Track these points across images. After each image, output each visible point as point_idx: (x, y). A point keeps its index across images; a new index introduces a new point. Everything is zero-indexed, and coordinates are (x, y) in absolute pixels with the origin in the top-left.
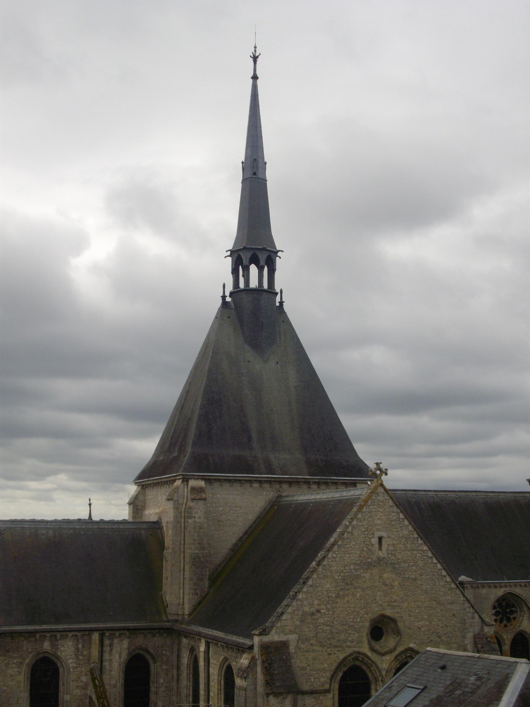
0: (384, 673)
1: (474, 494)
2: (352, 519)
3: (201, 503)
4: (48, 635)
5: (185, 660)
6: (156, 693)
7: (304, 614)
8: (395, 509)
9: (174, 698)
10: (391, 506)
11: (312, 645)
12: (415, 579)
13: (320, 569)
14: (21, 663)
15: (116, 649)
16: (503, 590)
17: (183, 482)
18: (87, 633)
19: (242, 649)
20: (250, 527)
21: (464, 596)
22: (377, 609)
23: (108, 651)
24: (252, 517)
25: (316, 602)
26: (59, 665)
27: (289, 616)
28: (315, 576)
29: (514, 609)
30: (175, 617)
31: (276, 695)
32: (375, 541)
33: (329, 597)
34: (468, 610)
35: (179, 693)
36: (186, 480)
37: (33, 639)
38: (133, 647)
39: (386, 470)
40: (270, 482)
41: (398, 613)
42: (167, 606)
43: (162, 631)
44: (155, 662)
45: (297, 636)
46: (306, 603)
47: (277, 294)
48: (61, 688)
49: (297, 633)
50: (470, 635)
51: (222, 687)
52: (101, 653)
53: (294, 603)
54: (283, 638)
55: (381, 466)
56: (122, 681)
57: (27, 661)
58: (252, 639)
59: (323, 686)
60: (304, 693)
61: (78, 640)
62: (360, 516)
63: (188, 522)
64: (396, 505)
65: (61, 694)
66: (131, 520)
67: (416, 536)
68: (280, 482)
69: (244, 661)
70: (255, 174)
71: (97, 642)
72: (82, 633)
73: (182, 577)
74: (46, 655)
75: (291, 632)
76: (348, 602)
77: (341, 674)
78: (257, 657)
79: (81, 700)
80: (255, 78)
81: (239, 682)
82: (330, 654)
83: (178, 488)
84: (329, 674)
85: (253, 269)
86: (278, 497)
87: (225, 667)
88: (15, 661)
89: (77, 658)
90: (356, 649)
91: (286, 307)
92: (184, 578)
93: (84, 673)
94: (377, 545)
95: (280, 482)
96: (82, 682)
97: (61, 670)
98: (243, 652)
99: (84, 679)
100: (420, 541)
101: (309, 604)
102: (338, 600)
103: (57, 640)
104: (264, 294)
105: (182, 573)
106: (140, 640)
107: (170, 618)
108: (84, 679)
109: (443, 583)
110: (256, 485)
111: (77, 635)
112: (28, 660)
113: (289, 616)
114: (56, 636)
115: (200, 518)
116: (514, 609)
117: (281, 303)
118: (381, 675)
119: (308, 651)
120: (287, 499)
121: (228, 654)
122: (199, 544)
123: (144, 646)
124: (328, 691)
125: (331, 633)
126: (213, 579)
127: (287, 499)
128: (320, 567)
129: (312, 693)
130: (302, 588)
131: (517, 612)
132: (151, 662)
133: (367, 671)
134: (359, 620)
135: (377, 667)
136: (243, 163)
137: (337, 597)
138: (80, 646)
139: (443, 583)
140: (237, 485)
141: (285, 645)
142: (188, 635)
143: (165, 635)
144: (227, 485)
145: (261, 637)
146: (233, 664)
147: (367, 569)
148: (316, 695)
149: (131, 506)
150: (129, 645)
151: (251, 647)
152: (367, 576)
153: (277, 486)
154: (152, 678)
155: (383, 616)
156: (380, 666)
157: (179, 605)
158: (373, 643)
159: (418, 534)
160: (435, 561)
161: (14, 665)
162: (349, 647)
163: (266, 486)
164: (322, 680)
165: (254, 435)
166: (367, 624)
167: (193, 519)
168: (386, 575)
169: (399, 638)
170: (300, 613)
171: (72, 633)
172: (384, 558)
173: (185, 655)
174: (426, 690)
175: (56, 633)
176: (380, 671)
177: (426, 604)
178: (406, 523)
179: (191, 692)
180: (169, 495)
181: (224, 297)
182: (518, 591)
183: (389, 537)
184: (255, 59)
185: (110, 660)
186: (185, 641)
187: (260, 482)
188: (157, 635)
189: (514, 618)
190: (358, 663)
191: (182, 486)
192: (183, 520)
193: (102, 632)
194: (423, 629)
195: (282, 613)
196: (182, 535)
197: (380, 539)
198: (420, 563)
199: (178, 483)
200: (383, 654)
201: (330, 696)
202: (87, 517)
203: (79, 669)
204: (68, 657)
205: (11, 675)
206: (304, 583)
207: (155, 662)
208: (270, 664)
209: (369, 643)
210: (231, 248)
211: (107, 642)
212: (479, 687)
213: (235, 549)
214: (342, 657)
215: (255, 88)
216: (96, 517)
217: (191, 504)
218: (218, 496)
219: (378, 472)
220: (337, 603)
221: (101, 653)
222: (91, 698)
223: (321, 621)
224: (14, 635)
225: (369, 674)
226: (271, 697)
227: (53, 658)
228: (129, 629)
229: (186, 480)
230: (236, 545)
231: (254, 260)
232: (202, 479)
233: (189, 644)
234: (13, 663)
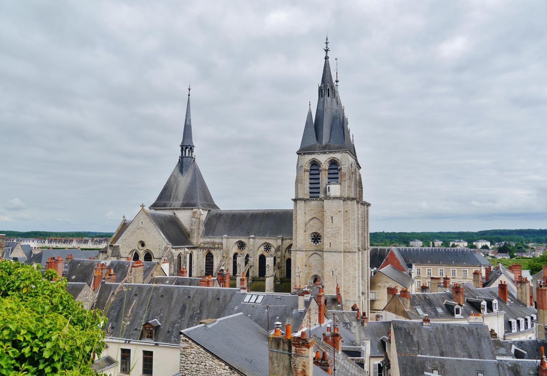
7: (123, 239)
50: (164, 247)
54: (118, 245)
75: (120, 243)
80: (189, 95)
104: (184, 158)
141: (118, 246)
152: (138, 231)
165: (172, 197)
168: (142, 231)
182: (243, 240)
184: (189, 89)
189: (244, 249)
198: (152, 228)
215: (189, 98)
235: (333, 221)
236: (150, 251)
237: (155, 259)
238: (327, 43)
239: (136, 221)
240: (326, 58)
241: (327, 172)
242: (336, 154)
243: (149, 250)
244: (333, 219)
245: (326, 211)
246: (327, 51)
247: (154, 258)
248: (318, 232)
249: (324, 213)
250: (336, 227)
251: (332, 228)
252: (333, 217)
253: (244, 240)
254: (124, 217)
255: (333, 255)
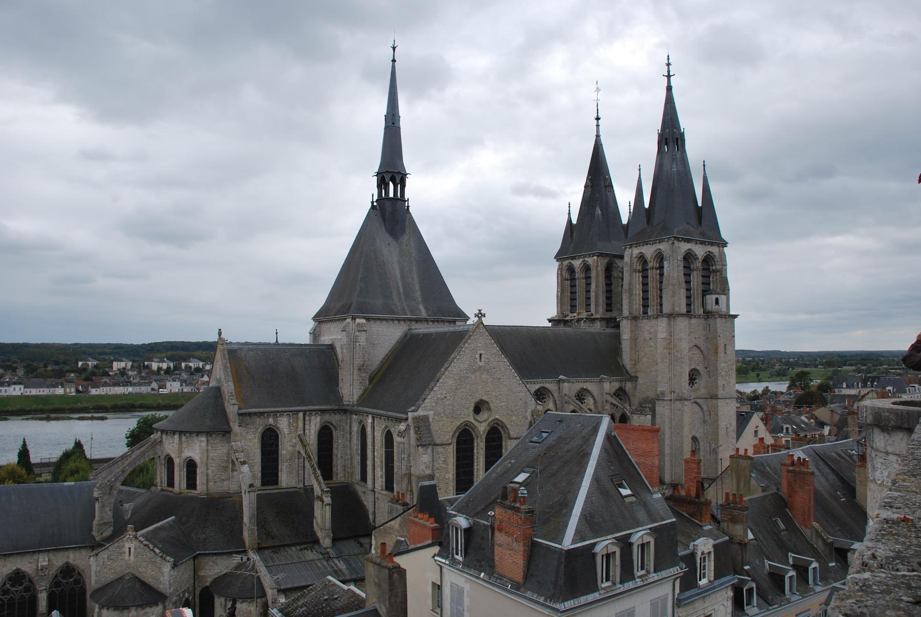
0: (482, 433)
1: (521, 328)
2: (465, 343)
3: (363, 333)
4: (272, 414)
5: (355, 428)
6: (337, 449)
7: (438, 399)
8: (490, 337)
9: (348, 451)
10: (487, 336)
11: (442, 417)
12: (499, 379)
13: (447, 373)
14: (256, 432)
15: (313, 422)
16: (539, 385)
17: (352, 320)
18: (295, 413)
19: (400, 420)
20: (392, 348)
21: (527, 388)
22: (478, 396)
23: (308, 424)
24: (393, 342)
25: (444, 392)
26: (278, 432)
27: (429, 401)
28: (444, 377)
29: (544, 396)
30: (348, 403)
31: (423, 446)
32: (478, 356)
33: (451, 389)
34: (528, 396)
35: (351, 448)
36: (354, 319)
37: (262, 417)
38: (323, 421)
39: (485, 314)
40: (404, 320)
41: (490, 398)
42: (343, 397)
43: (340, 411)
44: (336, 430)
45: (433, 412)
46: (438, 393)
47: (406, 201)
48: (280, 446)
49: (433, 410)
50: (529, 411)
51: (384, 443)
52: (304, 424)
53: (432, 393)
54: (426, 413)
55: (482, 312)
56: (316, 442)
57: (259, 430)
58: (407, 414)
59: (448, 440)
60: (438, 445)
61: (290, 417)
62: (469, 341)
63: (356, 345)
64: (490, 335)
65: (280, 450)
66: (312, 343)
67: (501, 353)
68: (411, 320)
69: (402, 427)
70: (393, 124)
71: (302, 418)
72: (293, 413)
73: (352, 378)
74: (271, 426)
75: (430, 410)
76: (462, 392)
77: (458, 434)
78: (411, 424)
79: (293, 453)
80: (394, 61)
81: (397, 439)
82: (452, 422)
83: (349, 323)
84: (451, 434)
85: (391, 185)
86: (409, 330)
87: (385, 431)
88: (252, 430)
89: (289, 428)
90: (467, 419)
91: (411, 209)
92: (353, 379)
93: (294, 437)
94: (479, 359)
95: (411, 320)
96: (293, 442)
97: (280, 436)
98: (401, 422)
99: (294, 441)
100: (503, 356)
101: (440, 393)
102: (457, 391)
103: (277, 417)
104: (399, 201)
105: (352, 376)
106: (327, 417)
107: (345, 403)
108: (294, 441)
109: (515, 381)
110: (396, 322)
111: (289, 414)
112: (260, 430)
113: (429, 401)
114: (276, 415)
115: (363, 342)
116: (544, 396)
117: (408, 207)
118: (480, 434)
119: (440, 421)
120: (416, 331)
121: (390, 423)
122: (362, 358)
123: (329, 421)
124: (450, 444)
125: (453, 410)
126: (371, 380)
127: (416, 331)
128: (447, 372)
129: (442, 445)
130: (436, 384)
131: (546, 398)
132: (333, 430)
133: (472, 432)
134: (468, 402)
135: (478, 429)
136: (385, 116)
137: (455, 389)
138: (291, 421)
139: (515, 381)
140: (384, 322)
141: (426, 418)
142: (357, 413)
143: (342, 414)
144: (378, 322)
145: (413, 413)
146: (392, 430)
147: (473, 373)
148: (444, 446)
149: (312, 335)
150: (321, 420)
151: (407, 419)
152: (473, 376)
153: (409, 323)
154: (334, 440)
155: (481, 400)
156: (479, 429)
157: (350, 395)
158: (475, 415)
159: (502, 352)
160: (511, 368)
161: (251, 433)
162: (463, 418)
163: (402, 323)
164: (447, 437)
166: (473, 405)
167: (359, 343)
168: (483, 376)
169: (490, 413)
170: (435, 398)
171: (287, 413)
172: (483, 366)
173: (355, 426)
174: (553, 432)
175: (276, 413)
176: (479, 432)
177: (506, 393)
178: (495, 345)
179: (360, 448)
180: (343, 328)
181: (372, 202)
182: (547, 386)
183: (485, 354)
184: (394, 48)
185: (310, 429)
186: (354, 416)
187: (399, 320)
188: (337, 414)
190: (467, 427)
191: (351, 323)
192: (352, 344)
193: (305, 412)
194: (504, 407)
195: (425, 399)
196: (352, 353)
197: (481, 355)
199: (349, 320)
200: (481, 422)
201: (452, 446)
202: (275, 341)
203: (291, 435)
204: (284, 428)
205: (250, 439)
206: (438, 381)
207: (336, 430)
208: (419, 428)
209: (474, 416)
210: (377, 171)
211: (307, 418)
212: (583, 430)
213: (383, 362)
214: (458, 424)
215: (393, 67)
216: (280, 342)
217: (357, 333)
218: (373, 329)
219: (480, 315)
220: (456, 392)
221: (304, 424)
222: (299, 452)
223: (447, 403)
224: (252, 415)
225: (473, 434)
226: (420, 447)
227: (274, 428)
228: (320, 411)
229: (354, 319)
230: (384, 359)
231: (393, 180)
232: (363, 318)
233: (358, 419)
234: (251, 432)
235: (727, 351)
236: (502, 422)
237: (512, 441)
238: (668, 65)
239: (467, 351)
240: (669, 88)
241: (700, 273)
242: (713, 247)
243: (500, 421)
244: (727, 348)
245: (721, 335)
246: (669, 76)
247: (511, 439)
248: (698, 368)
249: (718, 338)
250: (729, 361)
251: (726, 362)
252: (727, 346)
253: (551, 386)
254: (220, 334)
255: (727, 404)
